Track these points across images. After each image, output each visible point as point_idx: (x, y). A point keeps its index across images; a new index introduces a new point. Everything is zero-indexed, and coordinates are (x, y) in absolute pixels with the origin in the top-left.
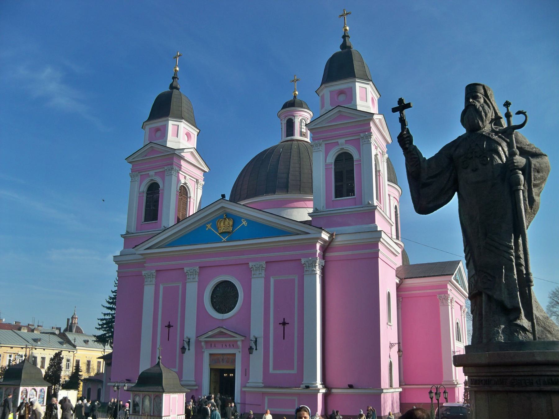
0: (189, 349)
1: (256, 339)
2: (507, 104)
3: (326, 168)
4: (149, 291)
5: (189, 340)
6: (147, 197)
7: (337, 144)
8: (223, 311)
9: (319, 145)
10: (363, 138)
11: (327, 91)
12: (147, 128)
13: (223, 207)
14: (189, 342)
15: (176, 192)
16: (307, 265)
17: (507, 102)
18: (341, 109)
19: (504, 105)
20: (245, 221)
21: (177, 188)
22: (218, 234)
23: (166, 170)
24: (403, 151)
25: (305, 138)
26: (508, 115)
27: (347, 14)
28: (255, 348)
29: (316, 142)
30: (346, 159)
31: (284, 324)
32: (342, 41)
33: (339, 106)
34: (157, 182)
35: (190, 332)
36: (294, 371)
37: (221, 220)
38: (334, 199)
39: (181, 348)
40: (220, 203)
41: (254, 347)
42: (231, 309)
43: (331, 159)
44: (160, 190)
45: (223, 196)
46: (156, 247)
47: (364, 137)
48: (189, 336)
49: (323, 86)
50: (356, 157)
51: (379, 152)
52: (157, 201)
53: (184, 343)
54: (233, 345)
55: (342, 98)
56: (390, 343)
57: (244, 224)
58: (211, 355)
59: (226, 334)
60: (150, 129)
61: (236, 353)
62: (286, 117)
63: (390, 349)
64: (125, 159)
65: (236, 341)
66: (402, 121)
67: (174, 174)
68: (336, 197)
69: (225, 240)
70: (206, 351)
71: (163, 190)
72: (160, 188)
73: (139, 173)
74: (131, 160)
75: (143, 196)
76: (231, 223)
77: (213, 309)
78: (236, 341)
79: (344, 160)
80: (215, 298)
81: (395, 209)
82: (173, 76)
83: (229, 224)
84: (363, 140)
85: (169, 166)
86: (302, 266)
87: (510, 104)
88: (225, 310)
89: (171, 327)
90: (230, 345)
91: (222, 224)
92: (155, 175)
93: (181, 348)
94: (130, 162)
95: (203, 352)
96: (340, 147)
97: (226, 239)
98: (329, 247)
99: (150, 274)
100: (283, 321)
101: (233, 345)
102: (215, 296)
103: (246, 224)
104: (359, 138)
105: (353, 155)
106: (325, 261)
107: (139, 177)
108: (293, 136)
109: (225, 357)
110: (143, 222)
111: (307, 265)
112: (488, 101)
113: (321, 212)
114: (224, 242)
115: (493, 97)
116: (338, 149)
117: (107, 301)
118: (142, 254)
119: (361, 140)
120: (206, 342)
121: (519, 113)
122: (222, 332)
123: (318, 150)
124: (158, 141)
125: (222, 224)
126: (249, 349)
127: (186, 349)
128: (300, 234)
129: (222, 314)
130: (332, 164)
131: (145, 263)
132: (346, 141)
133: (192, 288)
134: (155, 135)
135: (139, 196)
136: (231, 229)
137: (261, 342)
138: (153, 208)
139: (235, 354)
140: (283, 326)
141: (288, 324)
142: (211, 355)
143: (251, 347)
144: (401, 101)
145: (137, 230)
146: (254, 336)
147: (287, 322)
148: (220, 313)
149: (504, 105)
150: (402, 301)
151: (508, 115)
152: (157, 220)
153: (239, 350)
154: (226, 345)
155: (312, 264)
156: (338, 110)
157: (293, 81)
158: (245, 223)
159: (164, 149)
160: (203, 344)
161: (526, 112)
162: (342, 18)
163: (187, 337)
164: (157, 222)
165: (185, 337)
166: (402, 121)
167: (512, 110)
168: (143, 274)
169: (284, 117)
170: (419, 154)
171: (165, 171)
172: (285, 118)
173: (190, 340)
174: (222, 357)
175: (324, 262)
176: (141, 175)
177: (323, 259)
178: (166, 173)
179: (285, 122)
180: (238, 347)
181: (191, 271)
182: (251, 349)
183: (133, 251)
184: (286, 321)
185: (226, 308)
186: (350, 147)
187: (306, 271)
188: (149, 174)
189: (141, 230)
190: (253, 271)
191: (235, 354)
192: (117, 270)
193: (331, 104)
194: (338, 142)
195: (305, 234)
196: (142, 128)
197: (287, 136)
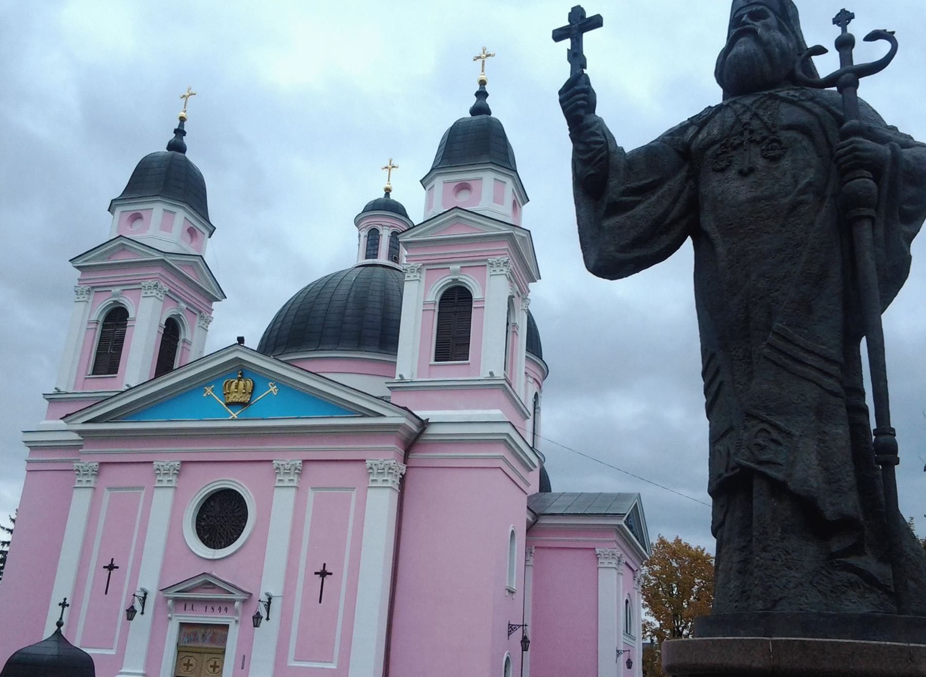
0: (142, 613)
1: (270, 599)
2: (843, 18)
3: (423, 310)
4: (81, 500)
5: (146, 594)
6: (102, 332)
8: (215, 543)
10: (492, 264)
11: (439, 182)
12: (118, 211)
13: (237, 359)
14: (144, 598)
15: (159, 329)
17: (843, 11)
18: (459, 213)
19: (836, 21)
20: (275, 387)
21: (160, 320)
22: (225, 406)
23: (144, 287)
24: (570, 129)
25: (397, 265)
26: (845, 44)
27: (488, 56)
28: (265, 616)
30: (459, 299)
31: (323, 574)
32: (473, 100)
34: (124, 307)
35: (150, 581)
36: (333, 666)
37: (232, 380)
38: (432, 362)
39: (127, 610)
40: (234, 351)
41: (264, 614)
42: (230, 541)
43: (434, 296)
44: (128, 322)
45: (241, 340)
46: (105, 421)
47: (494, 263)
48: (147, 588)
49: (435, 172)
50: (476, 295)
51: (517, 292)
52: (121, 340)
53: (134, 599)
54: (226, 609)
56: (509, 625)
57: (273, 390)
58: (182, 625)
59: (214, 586)
61: (228, 625)
62: (367, 226)
63: (509, 635)
64: (70, 261)
65: (232, 602)
66: (577, 58)
68: (436, 360)
69: (236, 417)
70: (174, 616)
71: (134, 320)
72: (128, 317)
74: (80, 263)
75: (96, 329)
77: (199, 539)
78: (232, 602)
79: (456, 299)
80: (204, 519)
81: (535, 398)
83: (244, 389)
84: (492, 269)
87: (851, 16)
88: (220, 543)
89: (114, 569)
90: (220, 607)
93: (127, 610)
94: (78, 268)
95: (170, 619)
97: (237, 415)
99: (87, 468)
100: (322, 569)
101: (226, 609)
102: (205, 516)
103: (275, 392)
104: (486, 266)
105: (471, 292)
106: (407, 467)
108: (376, 258)
109: (208, 631)
110: (89, 375)
113: (408, 382)
114: (233, 419)
116: (449, 279)
117: (11, 518)
118: (79, 432)
120: (176, 600)
121: (873, 36)
122: (210, 583)
124: (135, 236)
126: (253, 617)
127: (136, 612)
128: (369, 416)
129: (214, 550)
130: (435, 304)
132: (462, 267)
133: (163, 500)
135: (87, 329)
136: (246, 399)
137: (276, 606)
138: (112, 352)
139: (227, 626)
140: (321, 578)
141: (331, 574)
142: (182, 625)
143: (258, 613)
144: (577, 13)
145: (75, 387)
146: (267, 594)
147: (328, 572)
148: (210, 546)
149: (836, 21)
151: (845, 44)
152: (116, 373)
153: (237, 618)
154: (213, 609)
156: (455, 214)
157: (386, 168)
158: (274, 389)
160: (170, 602)
161: (893, 33)
162: (480, 61)
163: (142, 590)
164: (116, 377)
165: (138, 589)
166: (577, 58)
167: (859, 29)
170: (607, 139)
173: (147, 596)
174: (202, 630)
175: (405, 468)
176: (96, 292)
177: (404, 463)
180: (236, 612)
182: (257, 619)
183: (62, 424)
184: (328, 570)
185: (223, 539)
186: (467, 278)
189: (83, 389)
191: (227, 626)
193: (444, 205)
194: (449, 268)
195: (376, 416)
196: (109, 210)
197: (366, 258)
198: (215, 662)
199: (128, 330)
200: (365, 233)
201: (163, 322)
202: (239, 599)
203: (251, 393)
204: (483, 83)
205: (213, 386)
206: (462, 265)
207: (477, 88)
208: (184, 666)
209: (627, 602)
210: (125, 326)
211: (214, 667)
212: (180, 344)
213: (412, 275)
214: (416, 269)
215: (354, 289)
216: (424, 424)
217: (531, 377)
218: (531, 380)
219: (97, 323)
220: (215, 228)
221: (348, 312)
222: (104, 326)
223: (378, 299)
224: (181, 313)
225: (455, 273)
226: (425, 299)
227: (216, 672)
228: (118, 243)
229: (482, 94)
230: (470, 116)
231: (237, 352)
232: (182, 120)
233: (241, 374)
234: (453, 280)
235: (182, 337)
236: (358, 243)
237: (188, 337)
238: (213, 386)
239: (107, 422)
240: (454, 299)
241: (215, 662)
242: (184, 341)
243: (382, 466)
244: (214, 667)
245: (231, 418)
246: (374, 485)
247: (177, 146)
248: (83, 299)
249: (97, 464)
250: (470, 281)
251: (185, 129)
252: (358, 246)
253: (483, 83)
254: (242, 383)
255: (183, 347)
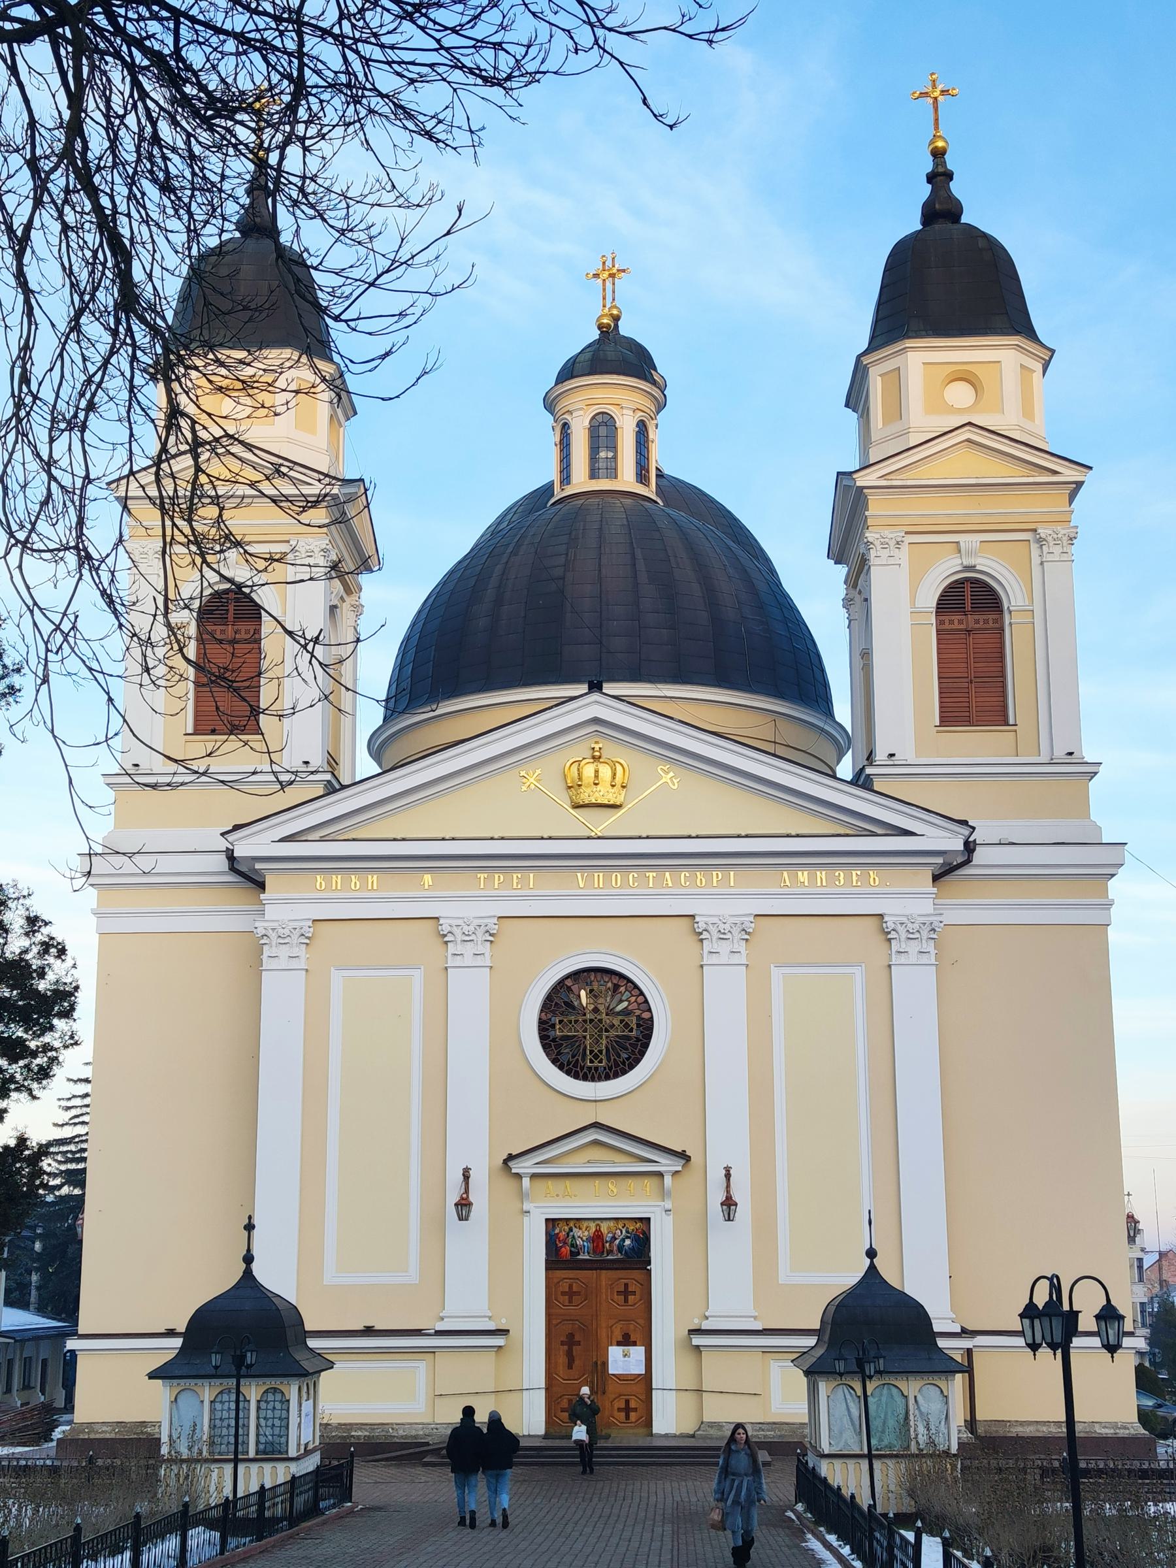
9: (892, 543)
13: (596, 721)
18: (966, 434)
20: (671, 774)
33: (970, 424)
43: (929, 598)
57: (669, 781)
61: (649, 1219)
65: (660, 1175)
99: (287, 932)
120: (534, 1176)
123: (891, 561)
129: (592, 1084)
139: (649, 1219)
160: (526, 1181)
181: (466, 929)
192: (95, 907)
198: (626, 1285)
202: (669, 1171)
204: (938, 155)
205: (538, 772)
207: (928, 165)
208: (561, 1298)
211: (626, 1293)
225: (970, 553)
227: (630, 1303)
229: (940, 177)
231: (596, 707)
238: (538, 772)
241: (626, 1285)
243: (916, 926)
244: (626, 1293)
246: (903, 961)
253: (938, 155)
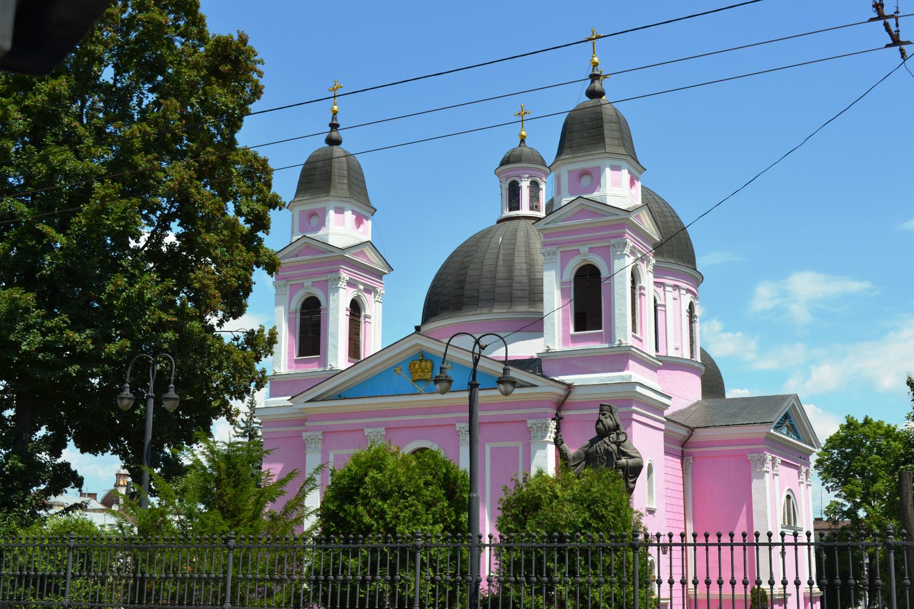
7: (577, 252)
13: (417, 345)
16: (535, 428)
29: (549, 248)
30: (590, 275)
33: (580, 197)
38: (572, 331)
43: (569, 275)
47: (616, 244)
50: (604, 274)
55: (586, 181)
60: (301, 212)
67: (343, 286)
68: (576, 330)
71: (327, 309)
72: (320, 305)
73: (287, 281)
76: (429, 365)
82: (331, 122)
84: (614, 249)
85: (334, 274)
86: (529, 431)
91: (417, 366)
92: (312, 286)
96: (583, 258)
98: (566, 401)
99: (313, 437)
104: (609, 246)
107: (288, 287)
108: (518, 209)
111: (535, 428)
112: (612, 416)
115: (617, 414)
119: (611, 248)
125: (417, 366)
130: (570, 282)
131: (305, 420)
134: (309, 223)
150: (692, 464)
155: (541, 427)
156: (579, 203)
157: (519, 114)
159: (327, 248)
168: (304, 437)
169: (505, 178)
171: (327, 280)
172: (506, 180)
176: (290, 285)
178: (330, 284)
179: (507, 186)
187: (534, 437)
188: (303, 283)
190: (461, 435)
197: (510, 210)
199: (321, 315)
200: (506, 186)
201: (348, 307)
203: (432, 371)
206: (590, 246)
209: (788, 497)
210: (319, 312)
212: (362, 319)
213: (549, 258)
214: (552, 253)
215: (502, 251)
216: (570, 387)
217: (683, 289)
218: (683, 292)
219: (296, 312)
220: (376, 210)
221: (499, 275)
222: (302, 314)
223: (523, 259)
224: (360, 294)
225: (584, 255)
226: (561, 278)
228: (303, 242)
230: (588, 99)
232: (335, 113)
233: (422, 356)
234: (584, 260)
235: (363, 314)
236: (500, 193)
237: (368, 312)
239: (323, 400)
240: (586, 275)
242: (366, 317)
245: (418, 392)
247: (333, 142)
248: (282, 292)
249: (321, 433)
250: (597, 261)
251: (339, 122)
252: (500, 196)
254: (423, 364)
255: (365, 322)
